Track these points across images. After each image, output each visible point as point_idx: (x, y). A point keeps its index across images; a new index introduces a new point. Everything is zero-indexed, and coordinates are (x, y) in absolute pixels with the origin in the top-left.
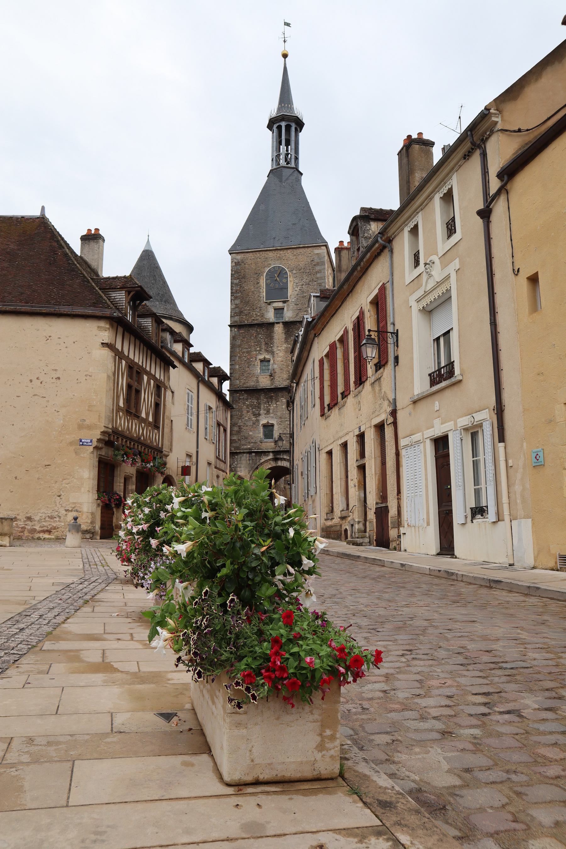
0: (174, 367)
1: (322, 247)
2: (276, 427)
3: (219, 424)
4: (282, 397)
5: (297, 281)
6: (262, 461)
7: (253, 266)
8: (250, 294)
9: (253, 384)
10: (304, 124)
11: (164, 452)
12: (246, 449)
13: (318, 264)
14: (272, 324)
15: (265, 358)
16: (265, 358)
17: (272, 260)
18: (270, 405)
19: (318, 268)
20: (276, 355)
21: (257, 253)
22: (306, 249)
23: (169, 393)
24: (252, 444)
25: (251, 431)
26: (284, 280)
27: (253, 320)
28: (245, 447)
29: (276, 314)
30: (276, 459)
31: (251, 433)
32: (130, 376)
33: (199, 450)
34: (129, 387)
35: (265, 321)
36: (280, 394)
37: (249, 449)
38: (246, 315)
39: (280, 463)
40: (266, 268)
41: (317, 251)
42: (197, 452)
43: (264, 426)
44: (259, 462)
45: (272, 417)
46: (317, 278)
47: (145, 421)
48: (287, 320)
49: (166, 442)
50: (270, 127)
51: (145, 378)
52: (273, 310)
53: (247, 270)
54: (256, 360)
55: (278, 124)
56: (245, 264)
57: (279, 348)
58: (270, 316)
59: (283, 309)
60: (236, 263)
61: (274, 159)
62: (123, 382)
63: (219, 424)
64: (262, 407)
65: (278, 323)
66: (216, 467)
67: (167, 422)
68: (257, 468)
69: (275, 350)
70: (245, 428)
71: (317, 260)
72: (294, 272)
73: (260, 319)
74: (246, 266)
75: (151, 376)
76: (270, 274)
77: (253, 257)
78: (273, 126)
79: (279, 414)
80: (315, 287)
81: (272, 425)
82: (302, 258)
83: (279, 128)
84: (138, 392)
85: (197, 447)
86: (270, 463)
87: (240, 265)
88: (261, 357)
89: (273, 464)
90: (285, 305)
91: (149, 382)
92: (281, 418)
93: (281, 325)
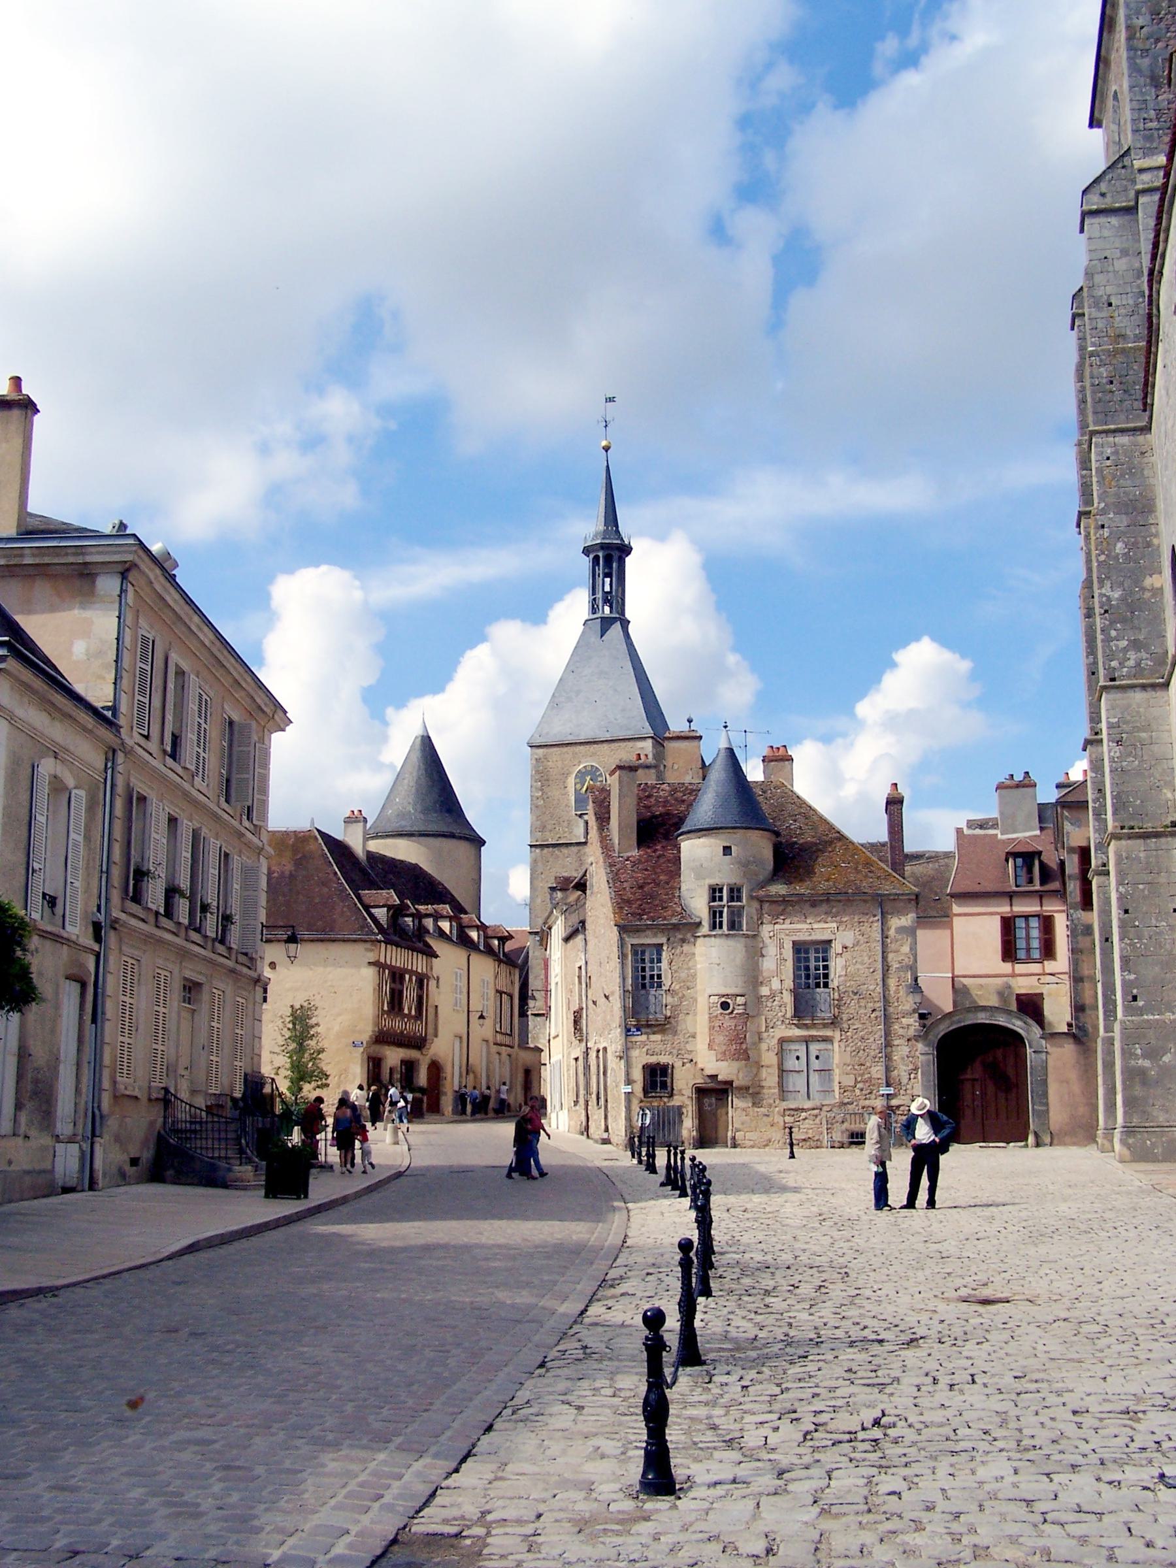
0: (437, 956)
3: (501, 993)
7: (559, 764)
23: (432, 983)
32: (393, 980)
34: (392, 991)
47: (409, 1016)
49: (430, 1031)
51: (407, 977)
62: (387, 988)
63: (500, 993)
66: (495, 1044)
67: (431, 1011)
75: (411, 972)
76: (581, 775)
84: (401, 992)
91: (410, 979)
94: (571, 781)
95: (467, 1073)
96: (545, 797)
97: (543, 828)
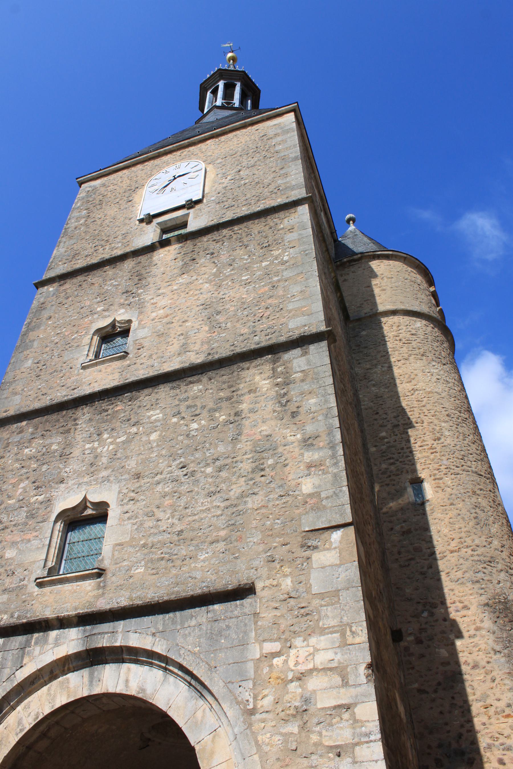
4: (153, 406)
10: (259, 91)
30: (93, 658)
36: (145, 397)
79: (132, 464)
89: (76, 685)
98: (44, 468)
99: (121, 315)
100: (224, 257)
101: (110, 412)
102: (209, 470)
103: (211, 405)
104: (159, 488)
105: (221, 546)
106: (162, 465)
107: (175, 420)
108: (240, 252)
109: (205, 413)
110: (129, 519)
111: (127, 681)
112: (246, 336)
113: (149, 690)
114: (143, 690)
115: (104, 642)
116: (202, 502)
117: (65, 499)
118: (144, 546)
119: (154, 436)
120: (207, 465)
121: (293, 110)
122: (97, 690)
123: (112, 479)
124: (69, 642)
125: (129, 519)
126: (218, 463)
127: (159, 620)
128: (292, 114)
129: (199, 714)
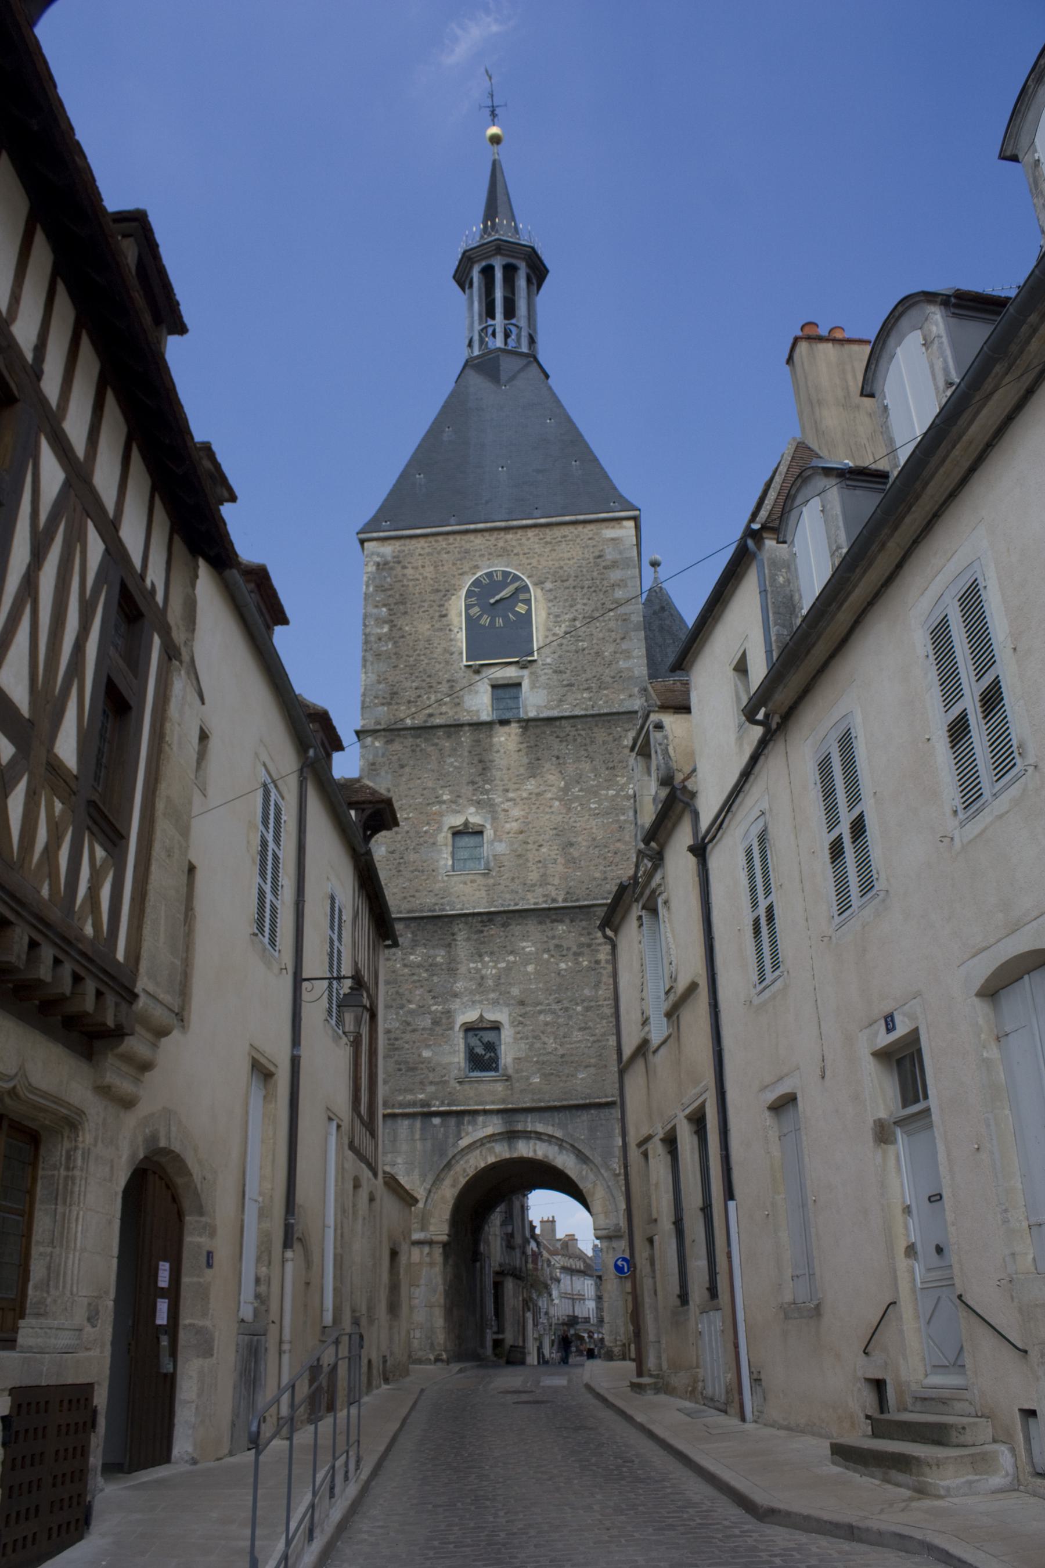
1: (626, 523)
2: (507, 1034)
4: (525, 937)
5: (555, 610)
6: (463, 1143)
7: (429, 571)
8: (421, 644)
9: (430, 900)
10: (547, 271)
11: (142, 1001)
12: (414, 1104)
13: (614, 564)
14: (489, 724)
15: (466, 824)
16: (466, 824)
17: (482, 556)
18: (485, 965)
19: (615, 575)
20: (502, 816)
21: (440, 538)
22: (580, 528)
24: (431, 1089)
25: (428, 1046)
26: (521, 608)
27: (431, 715)
28: (409, 1097)
29: (495, 699)
30: (511, 1136)
31: (426, 1054)
33: (304, 1052)
35: (465, 718)
36: (516, 929)
37: (425, 1104)
38: (409, 702)
39: (525, 1149)
40: (466, 577)
41: (610, 532)
42: (295, 1063)
43: (470, 1029)
44: (455, 1144)
45: (495, 1003)
46: (615, 601)
48: (532, 714)
50: (462, 279)
52: (489, 688)
53: (411, 584)
54: (439, 830)
55: (484, 264)
56: (404, 567)
57: (511, 795)
58: (480, 703)
59: (519, 685)
60: (378, 564)
61: (476, 338)
64: (463, 969)
65: (504, 722)
68: (448, 1165)
69: (498, 800)
70: (407, 1036)
71: (610, 555)
72: (548, 585)
73: (451, 714)
74: (409, 572)
77: (427, 550)
78: (471, 268)
79: (515, 991)
80: (612, 624)
81: (496, 1027)
82: (571, 548)
83: (488, 272)
85: (296, 1041)
86: (491, 1150)
87: (392, 569)
88: (458, 821)
89: (501, 1152)
90: (526, 673)
92: (522, 1003)
93: (514, 729)
94: (457, 607)
95: (287, 1244)
96: (396, 635)
97: (392, 697)
98: (436, 979)
99: (474, 817)
100: (570, 769)
101: (485, 934)
102: (579, 1008)
103: (574, 949)
104: (542, 1017)
105: (592, 1070)
106: (541, 996)
107: (546, 956)
108: (586, 766)
109: (571, 956)
110: (521, 1038)
111: (535, 1151)
112: (599, 882)
113: (551, 1157)
114: (547, 1157)
115: (520, 1127)
116: (577, 1035)
117: (464, 1013)
118: (537, 1062)
119: (530, 968)
120: (577, 1004)
121: (635, 519)
122: (515, 1155)
123: (501, 1002)
124: (493, 1126)
125: (521, 1038)
126: (585, 1004)
127: (557, 1117)
128: (631, 524)
129: (584, 1173)
